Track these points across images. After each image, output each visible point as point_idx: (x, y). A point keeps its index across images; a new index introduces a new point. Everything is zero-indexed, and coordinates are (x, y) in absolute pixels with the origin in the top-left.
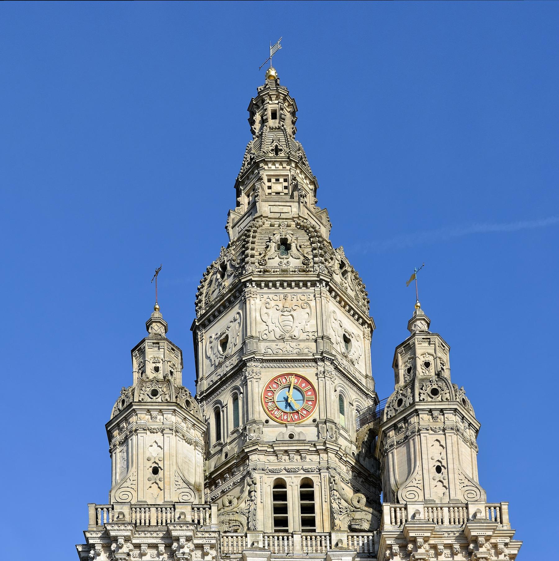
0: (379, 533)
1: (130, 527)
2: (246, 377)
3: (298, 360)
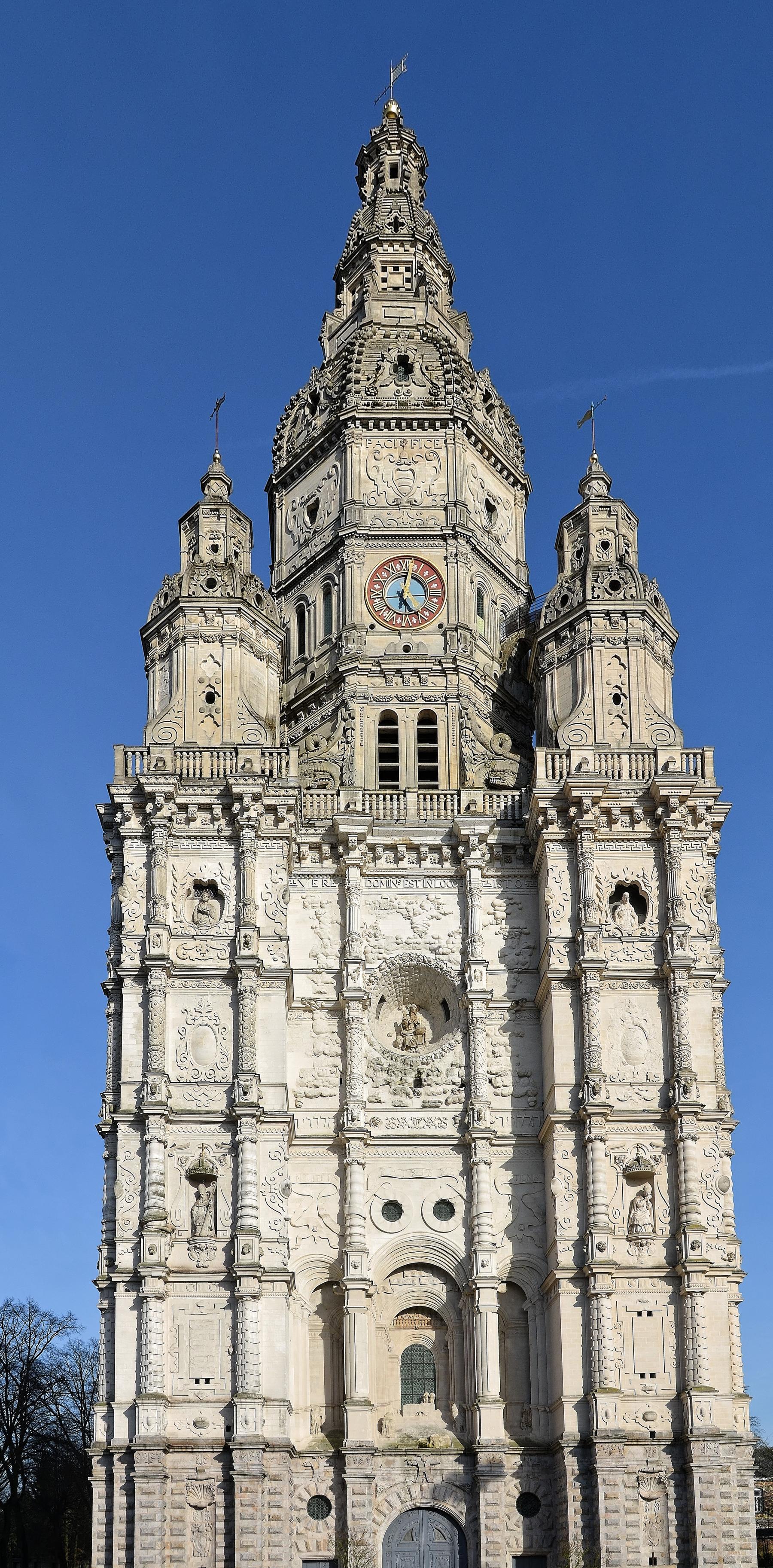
0: (529, 791)
1: (172, 780)
2: (343, 561)
3: (419, 536)
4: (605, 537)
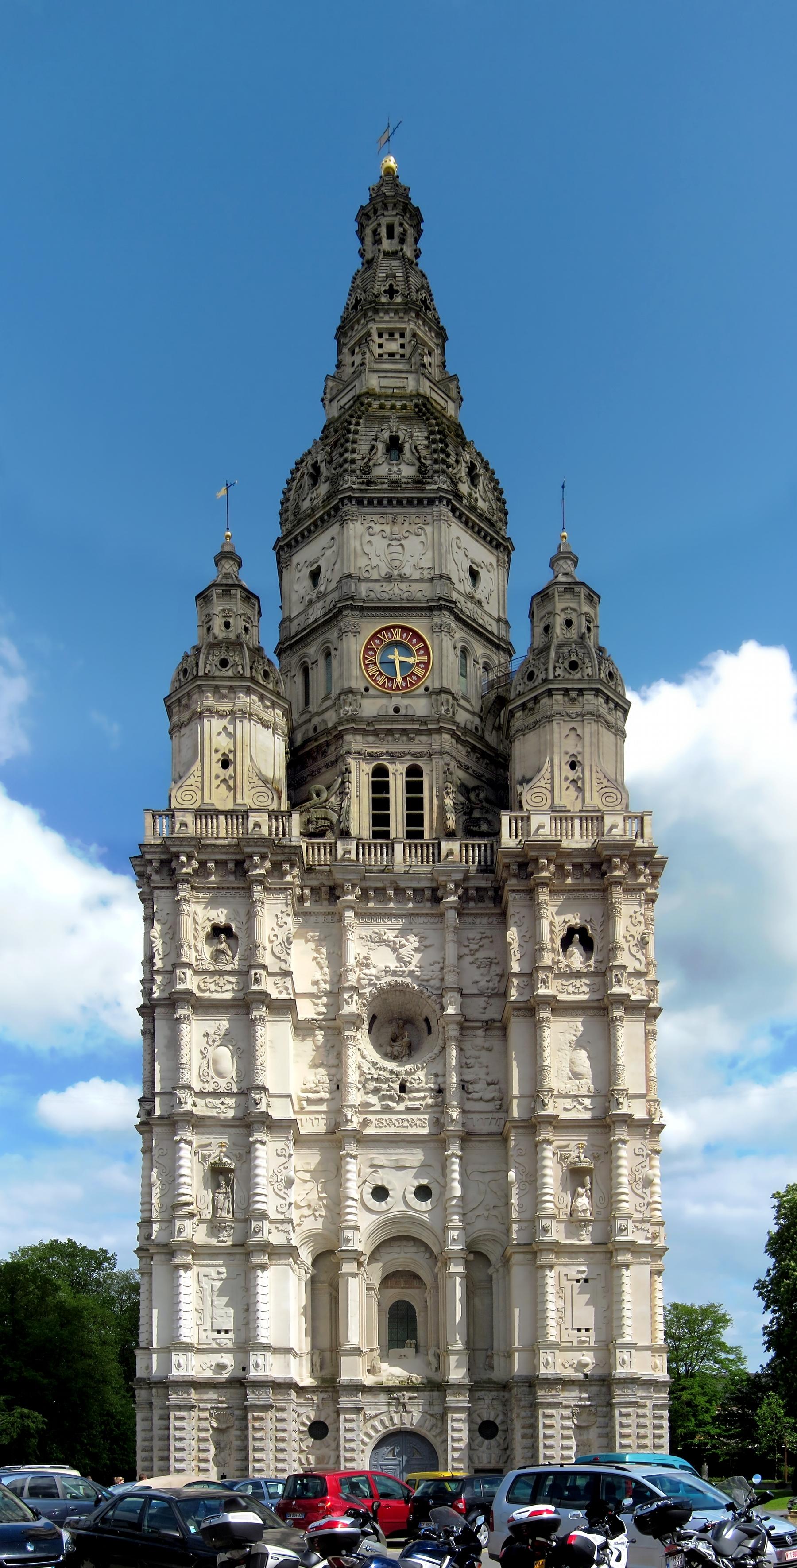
4: (569, 616)
